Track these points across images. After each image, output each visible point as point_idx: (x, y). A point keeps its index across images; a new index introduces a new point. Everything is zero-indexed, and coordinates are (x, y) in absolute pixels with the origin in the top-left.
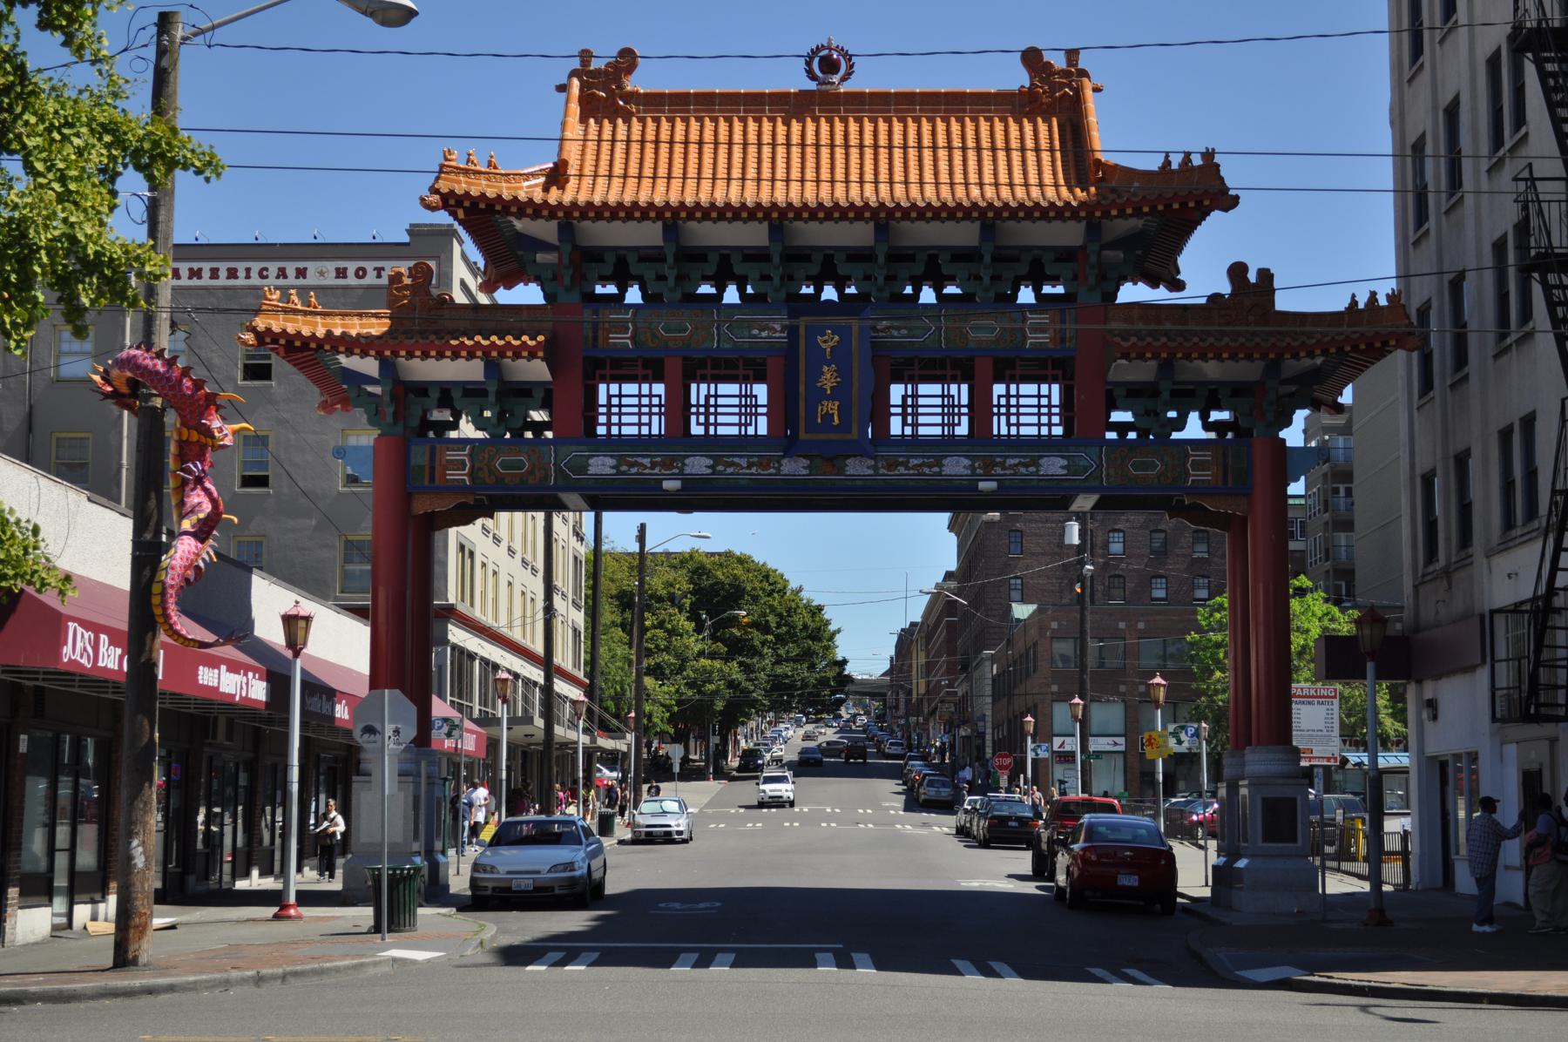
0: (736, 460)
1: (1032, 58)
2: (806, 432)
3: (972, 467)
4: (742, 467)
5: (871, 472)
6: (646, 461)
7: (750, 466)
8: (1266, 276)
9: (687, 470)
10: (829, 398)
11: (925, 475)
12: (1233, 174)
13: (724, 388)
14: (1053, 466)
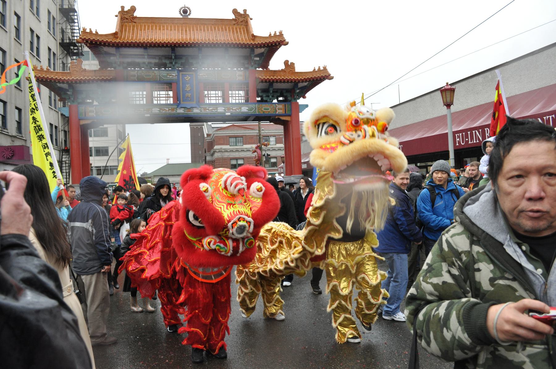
0: (165, 109)
1: (235, 11)
2: (183, 101)
3: (224, 110)
5: (200, 111)
7: (169, 110)
8: (293, 64)
9: (153, 112)
10: (188, 93)
12: (287, 38)
14: (245, 109)
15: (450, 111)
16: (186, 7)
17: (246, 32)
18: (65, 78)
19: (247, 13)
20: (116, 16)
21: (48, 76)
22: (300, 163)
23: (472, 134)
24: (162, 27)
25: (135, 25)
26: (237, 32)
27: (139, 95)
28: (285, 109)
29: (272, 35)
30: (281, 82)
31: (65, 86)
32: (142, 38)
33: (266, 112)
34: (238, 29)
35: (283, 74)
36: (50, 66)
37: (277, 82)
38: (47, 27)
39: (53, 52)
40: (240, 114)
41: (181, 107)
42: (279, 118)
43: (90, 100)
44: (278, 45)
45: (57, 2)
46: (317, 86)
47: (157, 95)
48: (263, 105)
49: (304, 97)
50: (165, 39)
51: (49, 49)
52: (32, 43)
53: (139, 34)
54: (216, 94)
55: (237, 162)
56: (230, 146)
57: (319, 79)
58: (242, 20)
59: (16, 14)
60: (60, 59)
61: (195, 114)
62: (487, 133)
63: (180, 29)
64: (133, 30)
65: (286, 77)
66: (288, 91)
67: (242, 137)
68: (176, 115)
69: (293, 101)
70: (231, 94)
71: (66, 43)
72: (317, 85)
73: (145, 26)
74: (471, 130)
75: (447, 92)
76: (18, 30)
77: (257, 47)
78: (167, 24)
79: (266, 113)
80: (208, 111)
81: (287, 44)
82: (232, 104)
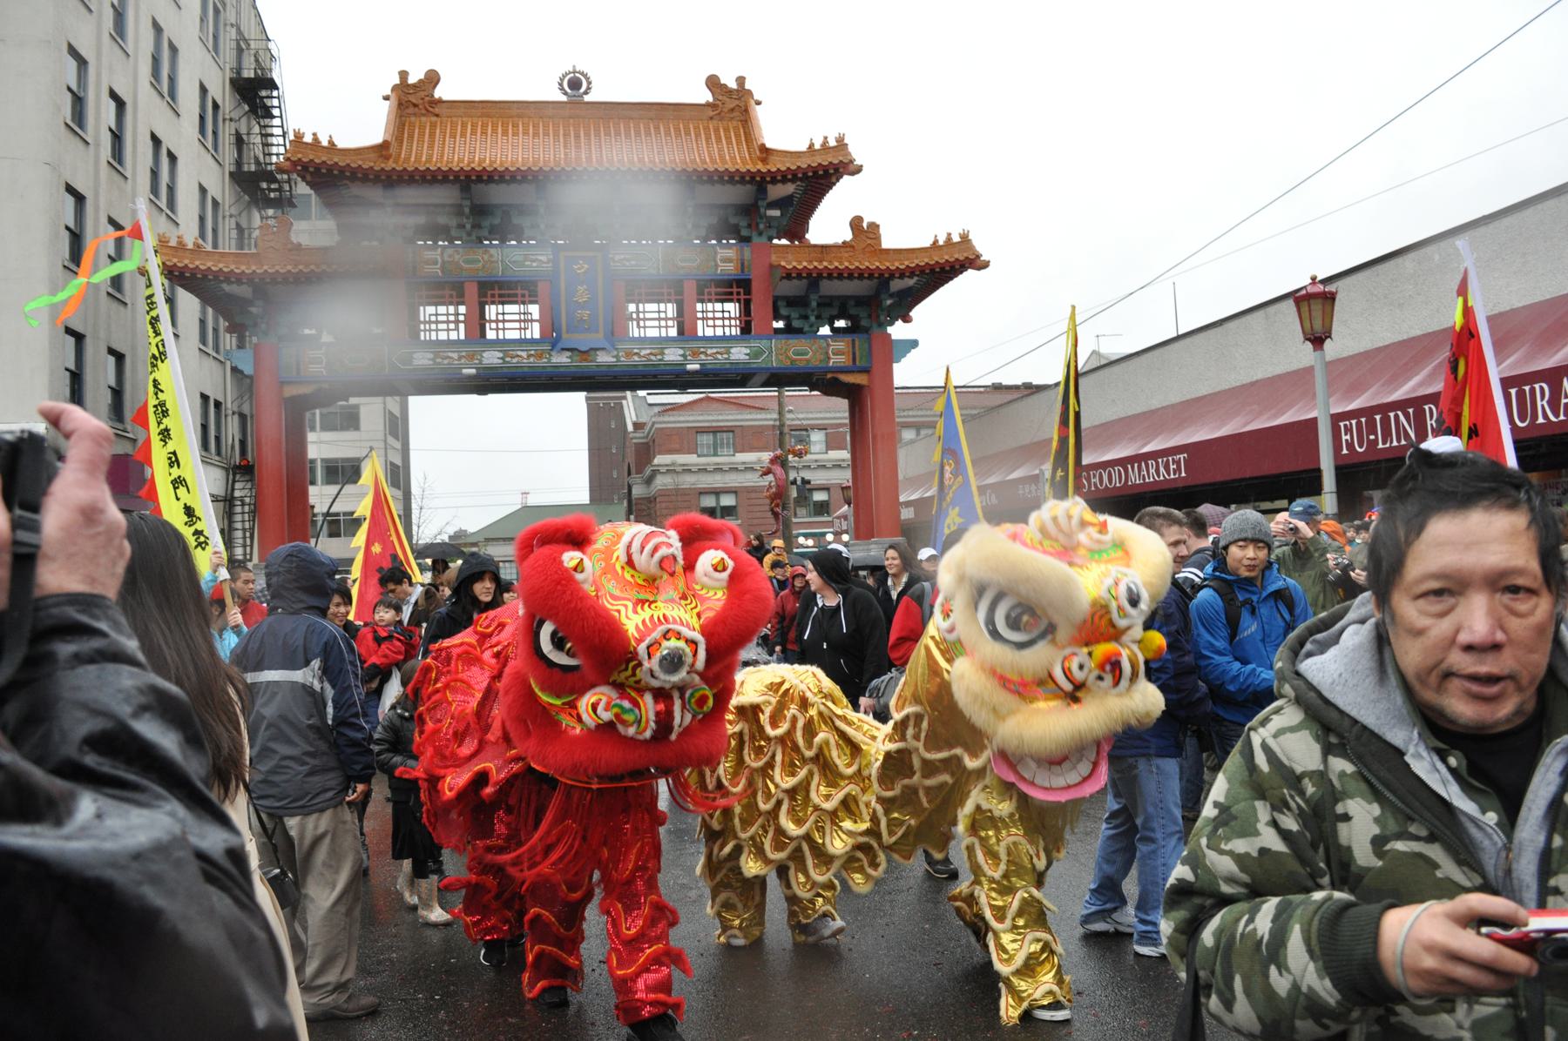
0: (519, 353)
1: (713, 83)
2: (568, 332)
4: (523, 359)
6: (455, 356)
7: (529, 356)
8: (874, 227)
11: (652, 360)
12: (858, 153)
13: (509, 308)
14: (739, 353)
15: (1323, 357)
16: (579, 72)
17: (743, 139)
18: (243, 268)
19: (747, 87)
20: (386, 98)
21: (197, 263)
22: (896, 505)
23: (1385, 421)
24: (510, 127)
25: (436, 122)
26: (719, 139)
27: (448, 315)
28: (854, 354)
29: (817, 146)
30: (840, 276)
31: (244, 291)
32: (456, 159)
33: (801, 360)
34: (721, 130)
35: (846, 255)
36: (202, 235)
37: (830, 277)
38: (197, 129)
39: (214, 201)
40: (728, 366)
41: (563, 349)
42: (836, 379)
43: (311, 329)
44: (831, 174)
45: (225, 62)
46: (942, 289)
47: (498, 314)
48: (791, 341)
49: (907, 319)
50: (520, 159)
51: (203, 190)
52: (155, 174)
53: (447, 148)
54: (659, 312)
55: (718, 500)
56: (699, 456)
57: (948, 268)
58: (732, 106)
59: (113, 95)
60: (231, 216)
61: (603, 369)
62: (1431, 419)
63: (561, 132)
64: (432, 135)
65: (857, 264)
66: (860, 301)
67: (733, 431)
68: (549, 370)
69: (875, 330)
70: (703, 312)
71: (250, 172)
72: (943, 285)
73: (464, 126)
74: (1384, 409)
75: (1312, 301)
76: (117, 137)
77: (774, 181)
78: (526, 120)
79: (802, 364)
80: (636, 358)
81: (859, 170)
82: (705, 338)
